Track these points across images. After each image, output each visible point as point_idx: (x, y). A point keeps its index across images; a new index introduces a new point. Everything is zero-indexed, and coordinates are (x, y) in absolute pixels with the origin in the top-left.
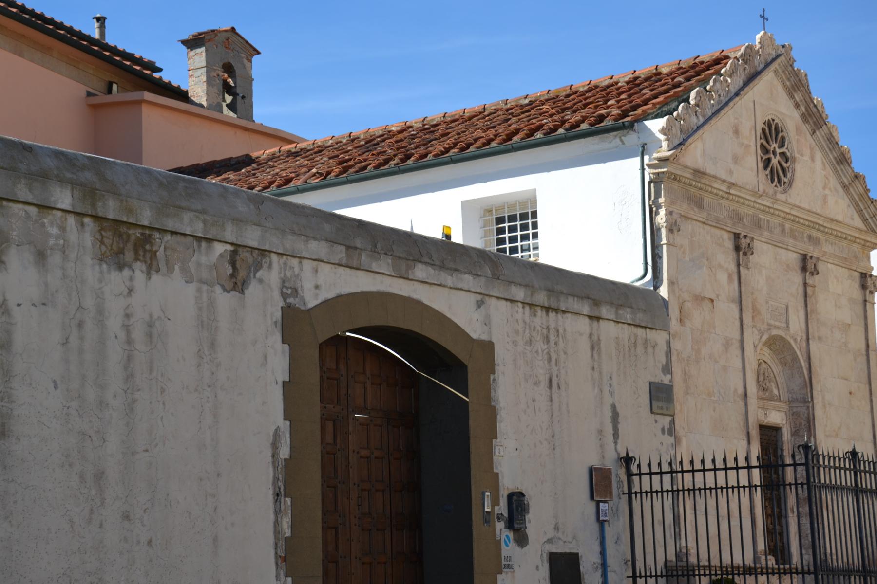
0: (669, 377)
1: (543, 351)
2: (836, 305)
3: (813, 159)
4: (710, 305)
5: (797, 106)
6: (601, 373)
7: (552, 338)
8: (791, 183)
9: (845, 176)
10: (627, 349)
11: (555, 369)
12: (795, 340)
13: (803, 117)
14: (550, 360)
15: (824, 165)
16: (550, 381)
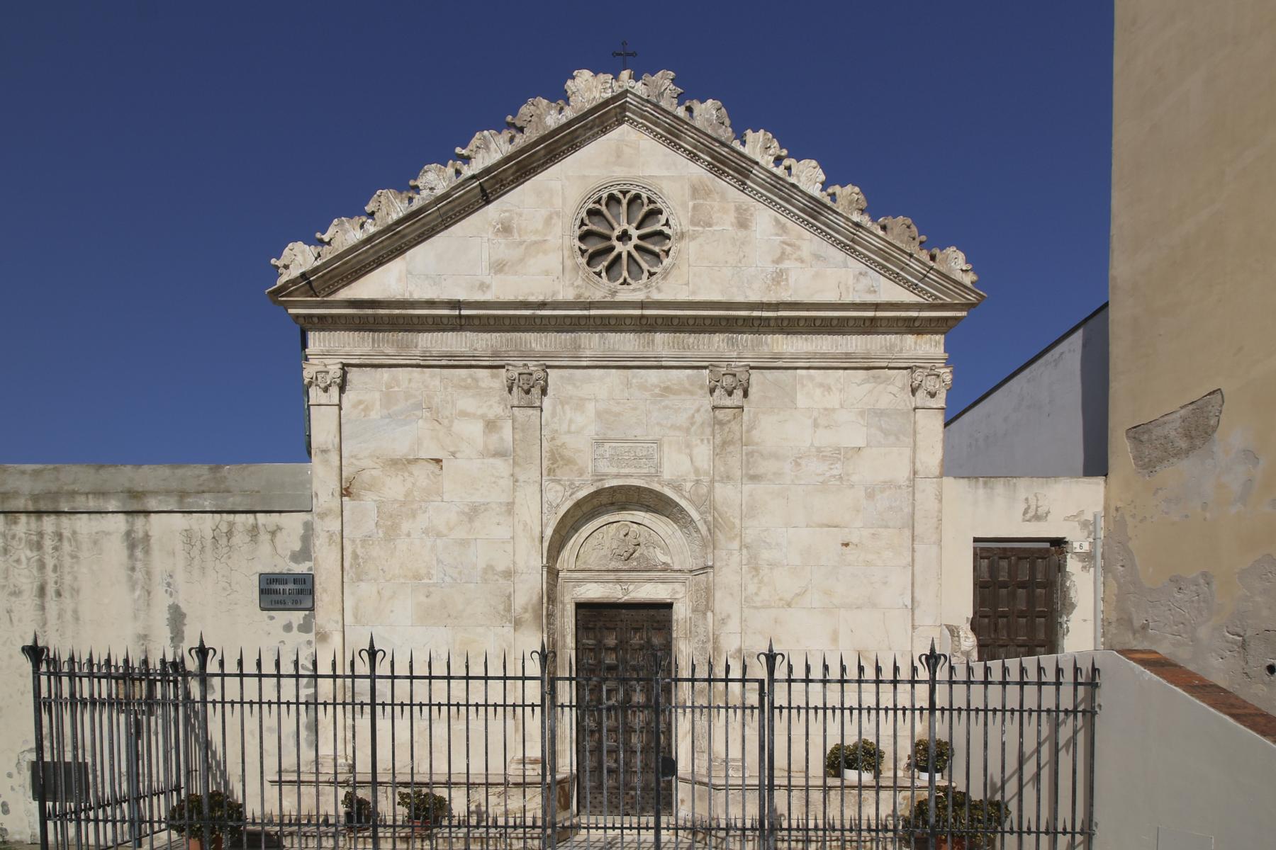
0: (308, 564)
1: (29, 559)
2: (816, 425)
3: (743, 224)
4: (433, 467)
5: (694, 157)
6: (148, 573)
7: (48, 543)
8: (666, 273)
9: (837, 232)
10: (209, 542)
11: (51, 577)
12: (678, 489)
13: (712, 168)
14: (42, 566)
15: (783, 227)
16: (42, 591)
